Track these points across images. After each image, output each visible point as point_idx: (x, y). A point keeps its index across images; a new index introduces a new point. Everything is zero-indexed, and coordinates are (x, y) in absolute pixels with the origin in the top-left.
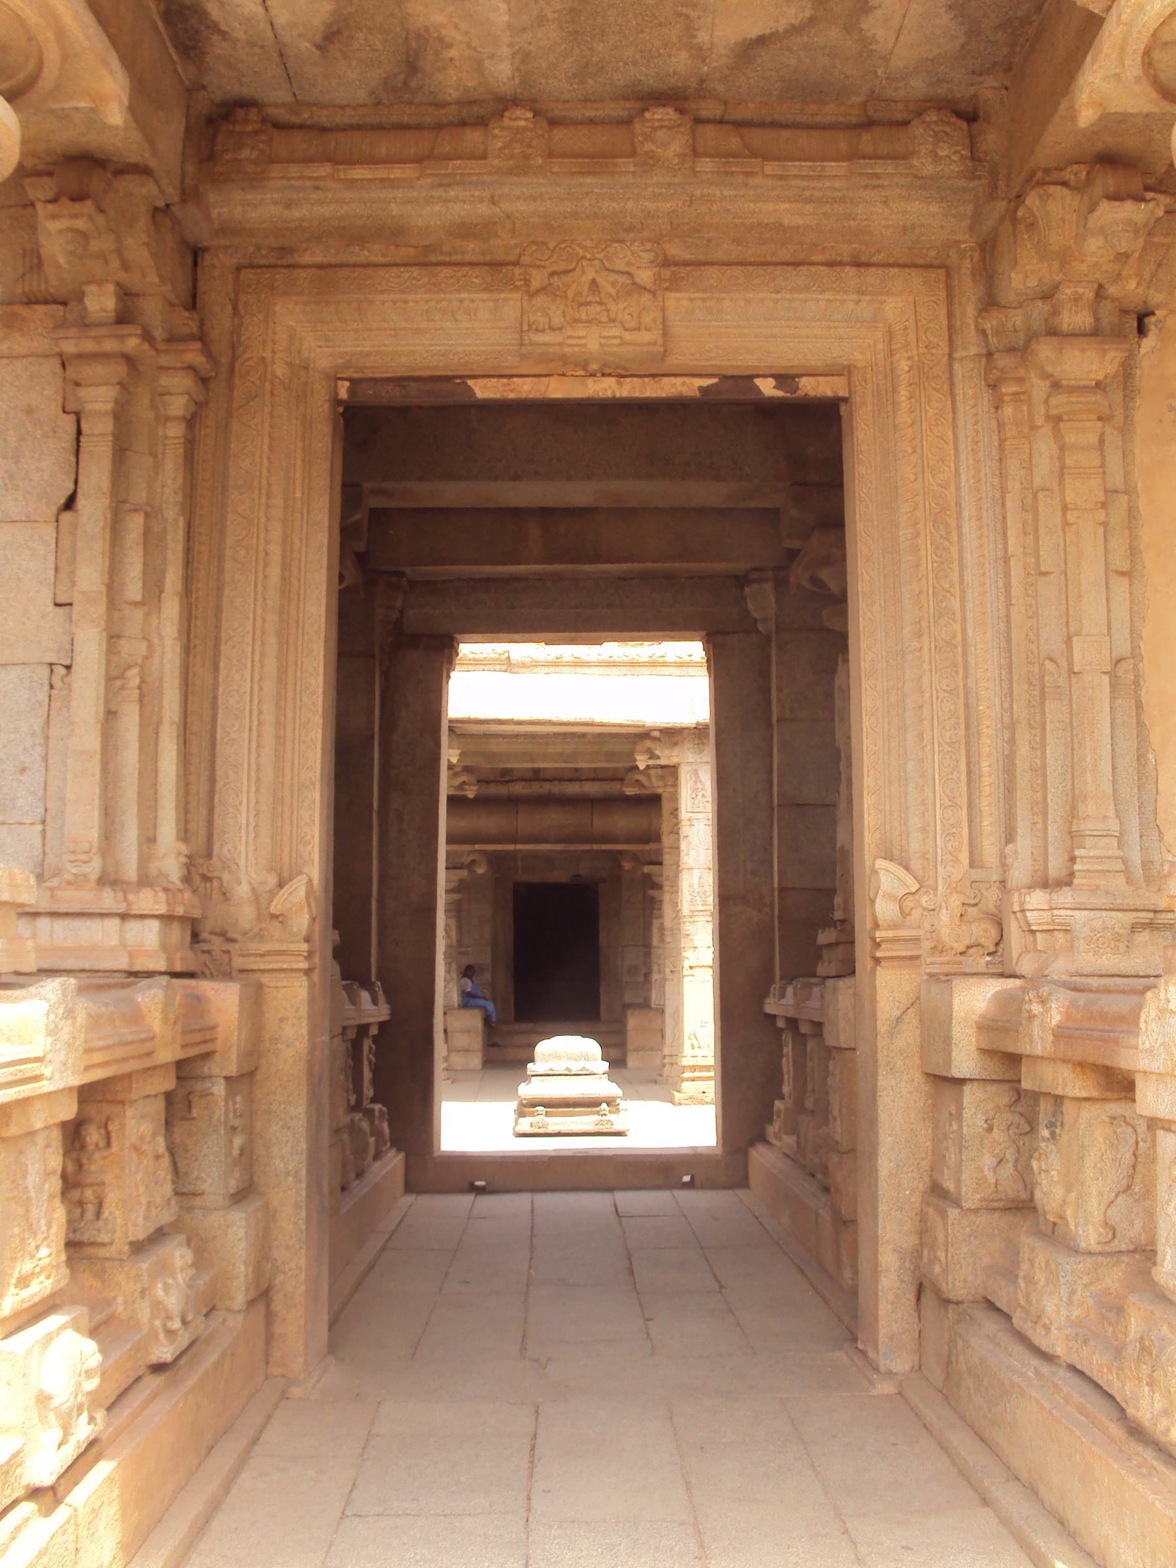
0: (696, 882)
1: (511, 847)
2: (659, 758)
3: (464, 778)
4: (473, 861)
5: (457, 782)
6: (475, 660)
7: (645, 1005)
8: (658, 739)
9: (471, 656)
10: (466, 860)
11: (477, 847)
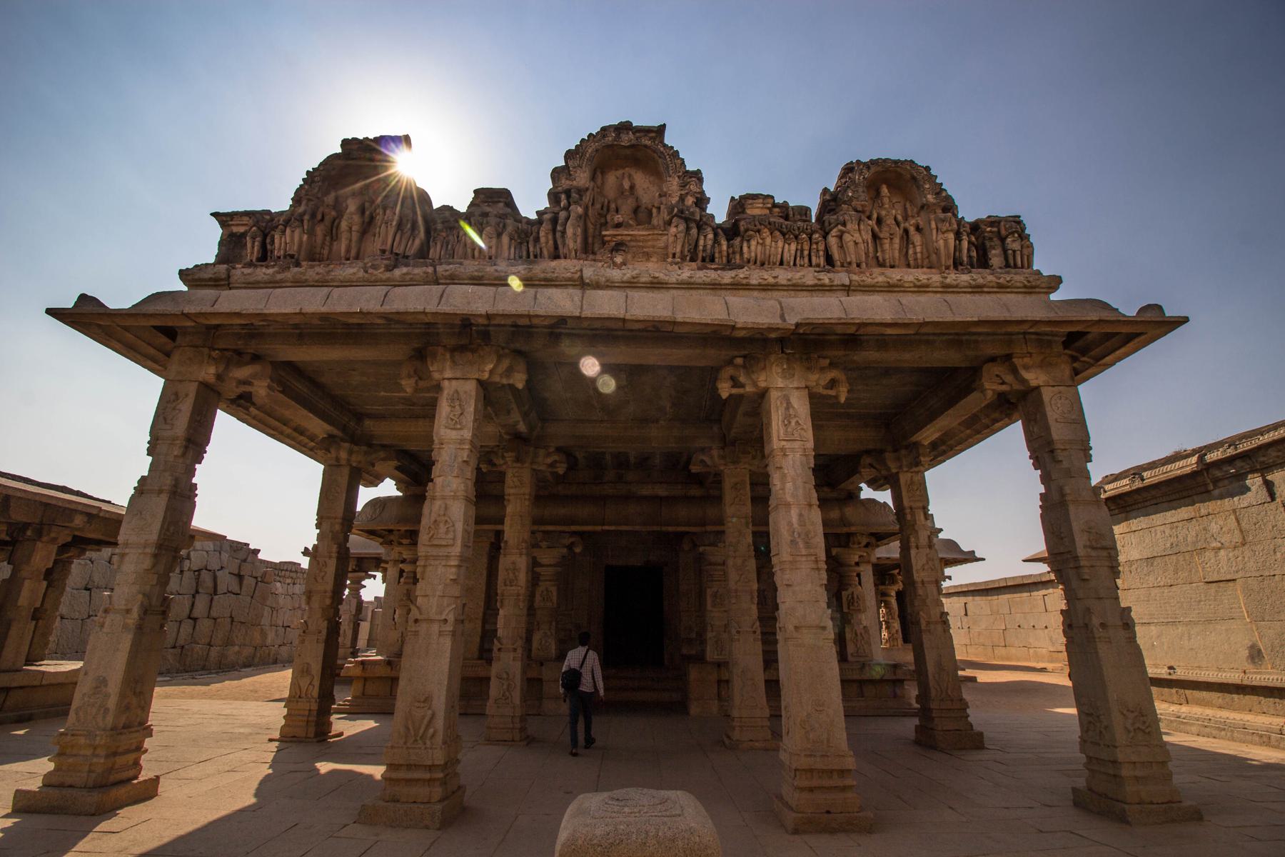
0: (795, 520)
1: (599, 528)
2: (743, 386)
3: (556, 457)
4: (572, 543)
5: (549, 460)
6: (545, 280)
7: (700, 659)
9: (542, 276)
10: (567, 541)
11: (574, 528)
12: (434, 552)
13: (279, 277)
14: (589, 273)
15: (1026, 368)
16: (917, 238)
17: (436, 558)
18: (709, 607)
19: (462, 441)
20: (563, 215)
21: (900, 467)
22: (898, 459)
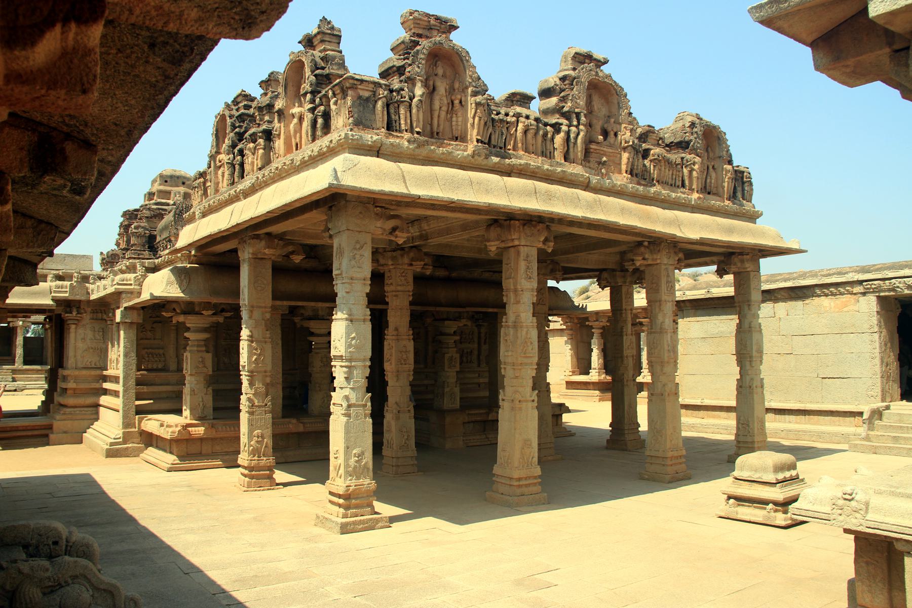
8: (647, 247)
12: (525, 360)
13: (418, 151)
14: (594, 180)
15: (748, 260)
16: (713, 175)
17: (526, 364)
18: (446, 369)
19: (532, 290)
20: (573, 129)
21: (625, 282)
22: (624, 277)
